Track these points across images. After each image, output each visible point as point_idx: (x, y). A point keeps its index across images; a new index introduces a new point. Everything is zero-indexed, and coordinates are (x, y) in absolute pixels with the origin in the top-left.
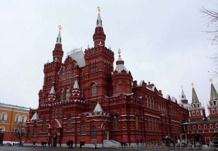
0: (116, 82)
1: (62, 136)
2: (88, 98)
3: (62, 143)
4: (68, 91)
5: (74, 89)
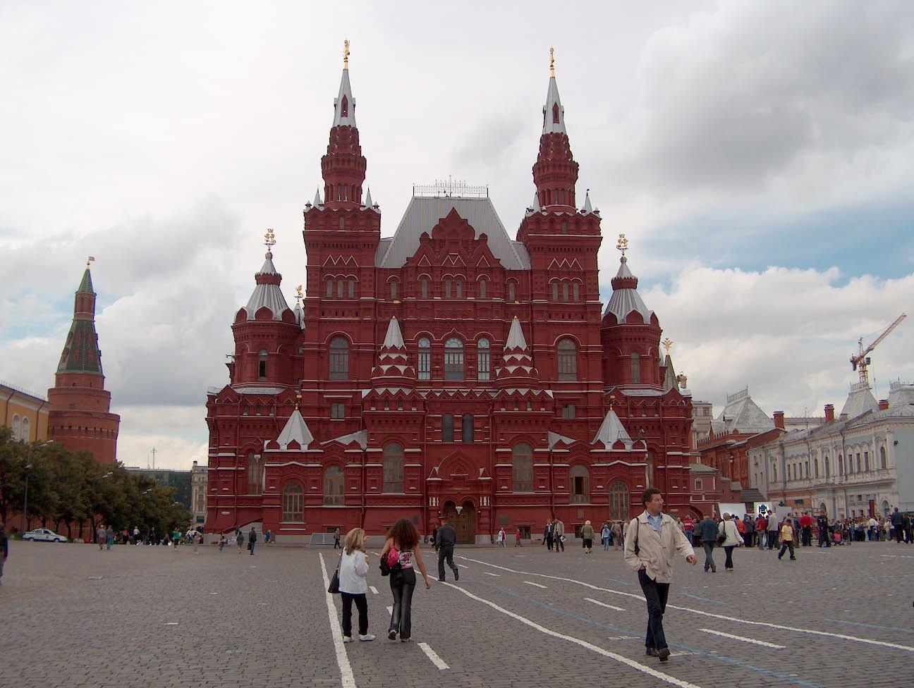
1: (495, 508)
3: (493, 530)
4: (454, 343)
5: (509, 351)
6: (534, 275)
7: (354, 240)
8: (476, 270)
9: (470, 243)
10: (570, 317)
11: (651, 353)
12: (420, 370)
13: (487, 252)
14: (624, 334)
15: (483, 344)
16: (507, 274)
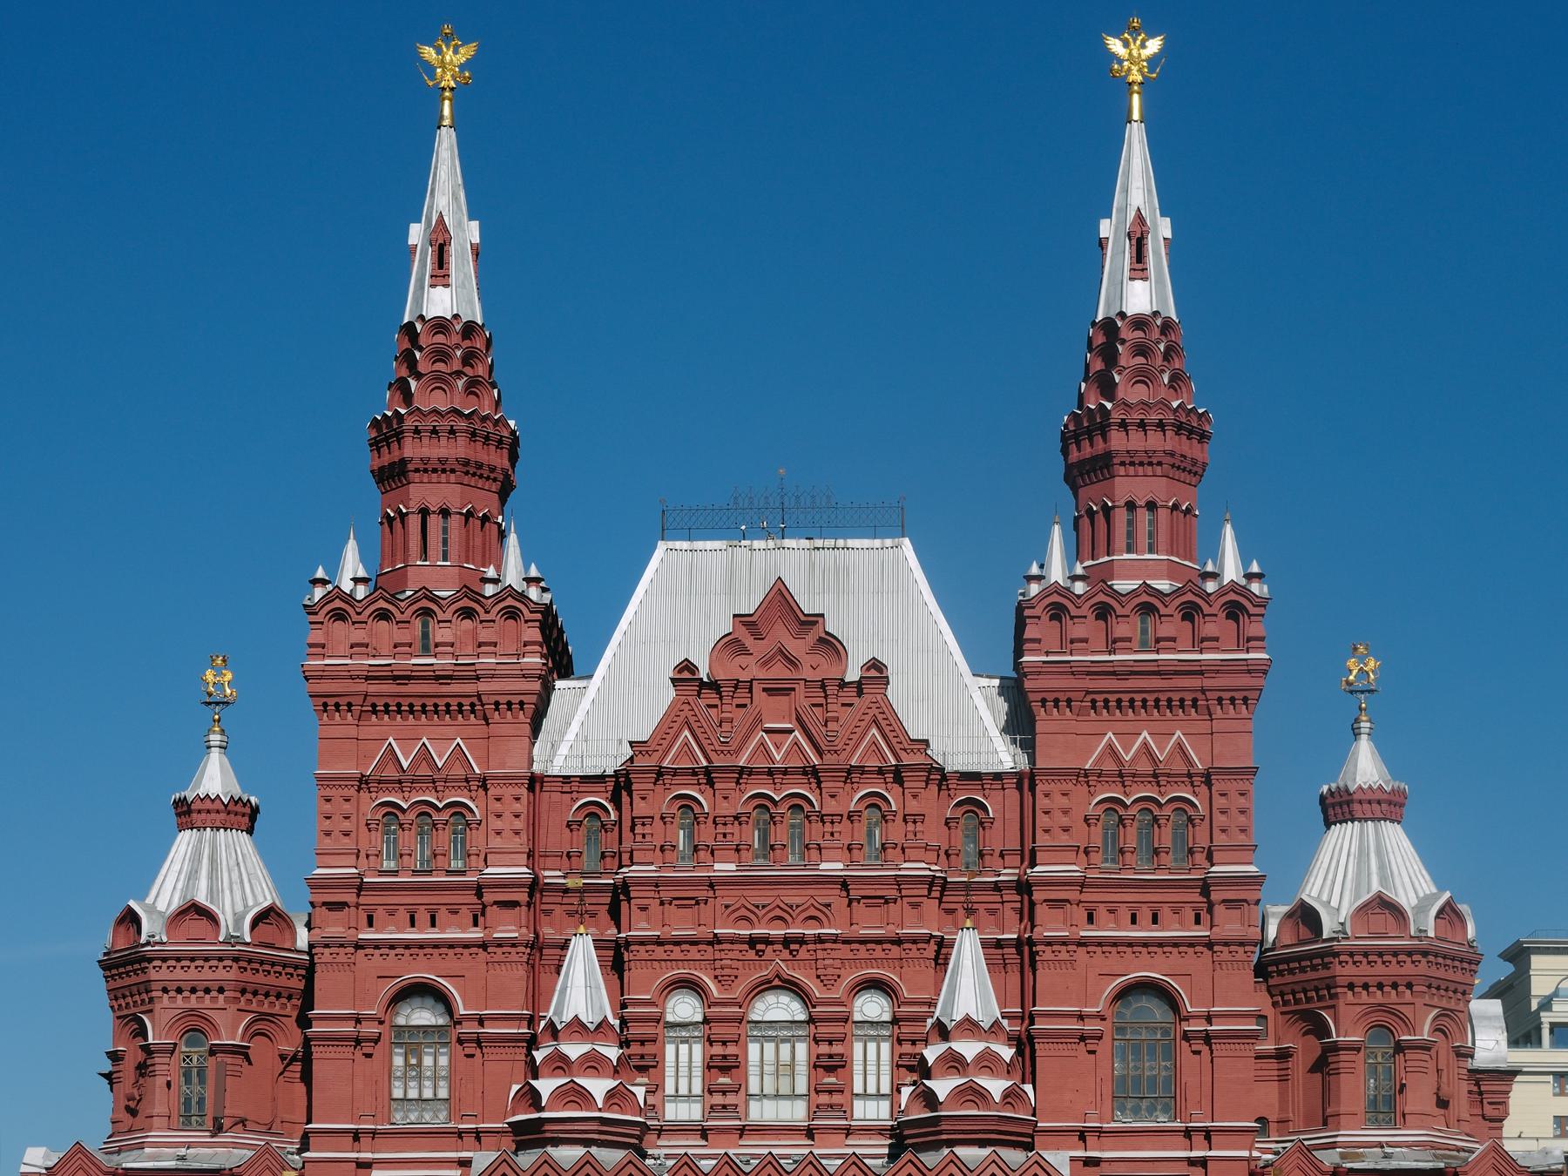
0: (1382, 1008)
2: (1082, 1135)
4: (779, 1007)
6: (1040, 788)
7: (469, 688)
8: (851, 774)
9: (831, 690)
10: (1155, 920)
11: (1438, 1029)
12: (669, 1089)
13: (886, 721)
14: (1344, 971)
15: (872, 1007)
16: (953, 784)
